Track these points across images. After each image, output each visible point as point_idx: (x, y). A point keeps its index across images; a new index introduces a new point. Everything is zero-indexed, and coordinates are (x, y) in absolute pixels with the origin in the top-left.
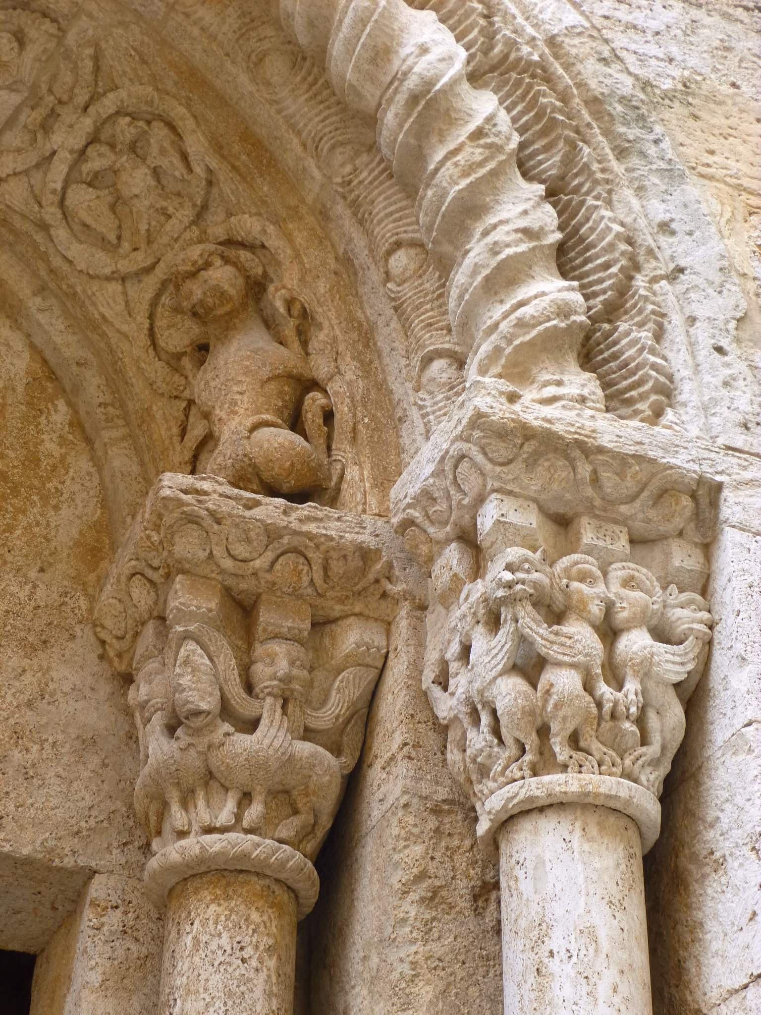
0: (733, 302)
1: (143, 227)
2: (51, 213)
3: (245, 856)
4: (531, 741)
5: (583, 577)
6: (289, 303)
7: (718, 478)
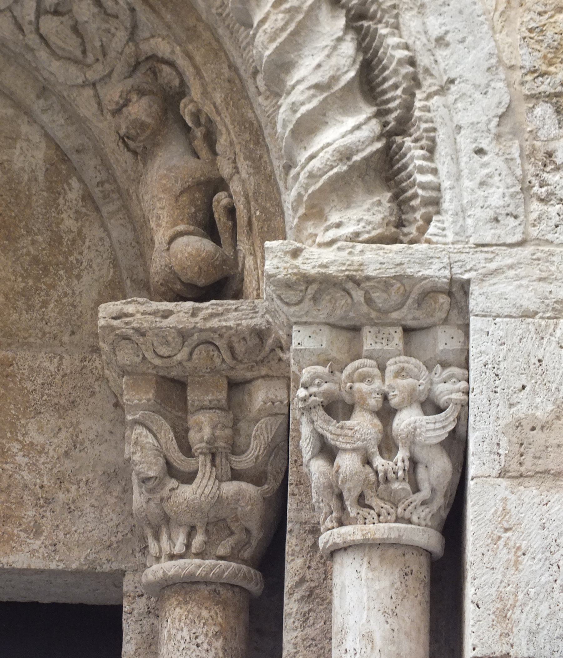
0: (496, 100)
1: (98, 44)
2: (32, 39)
3: (192, 575)
4: (334, 503)
5: (363, 378)
7: (466, 276)
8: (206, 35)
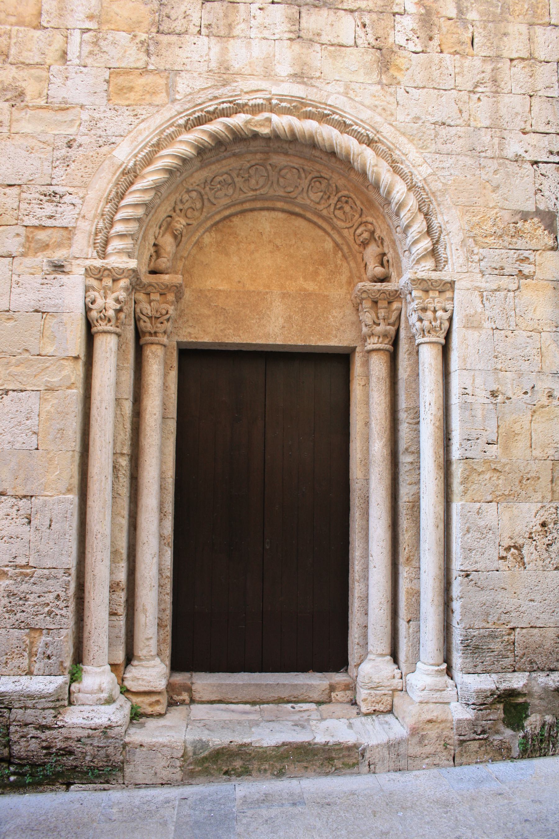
2: (332, 216)
6: (379, 237)
8: (382, 217)
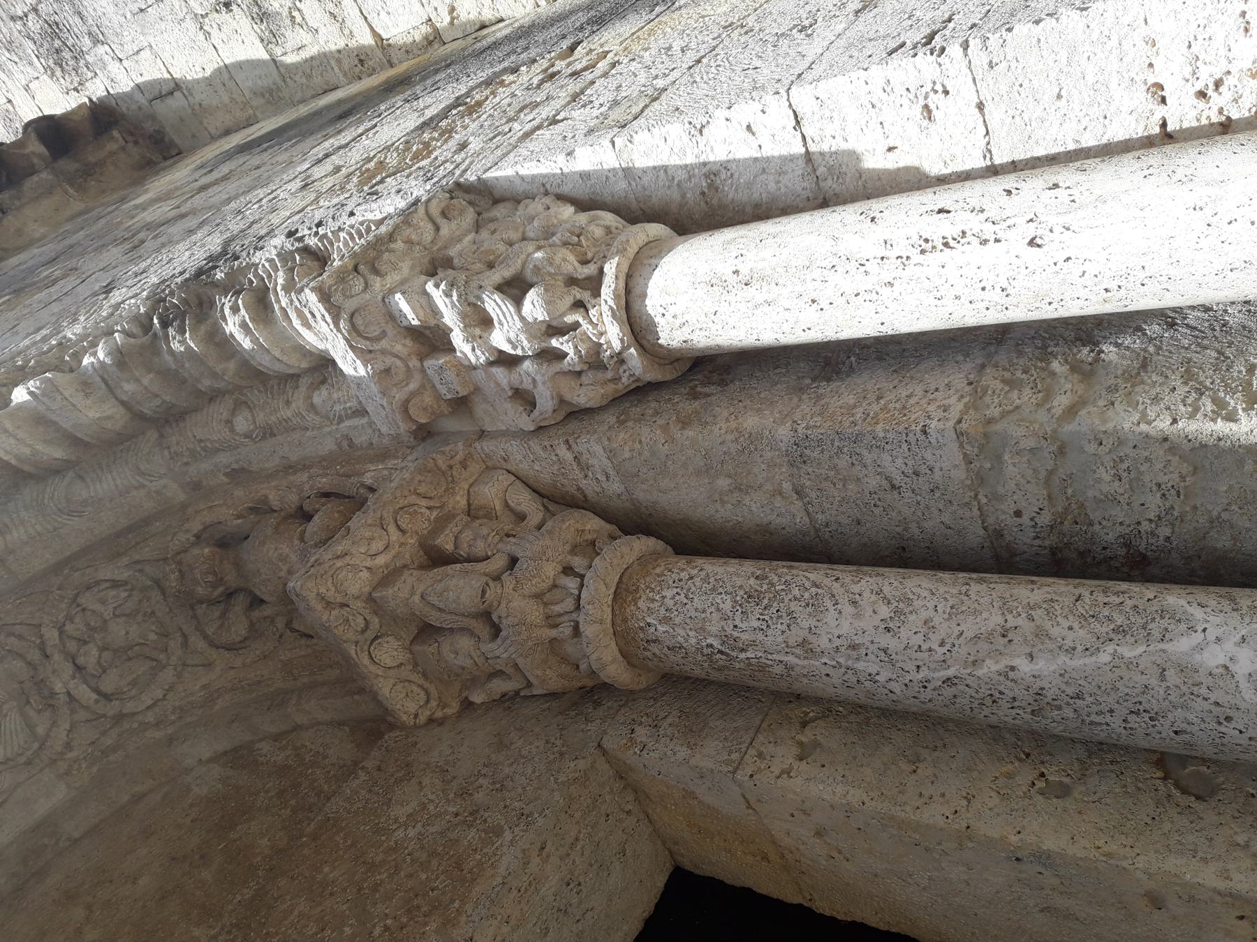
2: (111, 709)
